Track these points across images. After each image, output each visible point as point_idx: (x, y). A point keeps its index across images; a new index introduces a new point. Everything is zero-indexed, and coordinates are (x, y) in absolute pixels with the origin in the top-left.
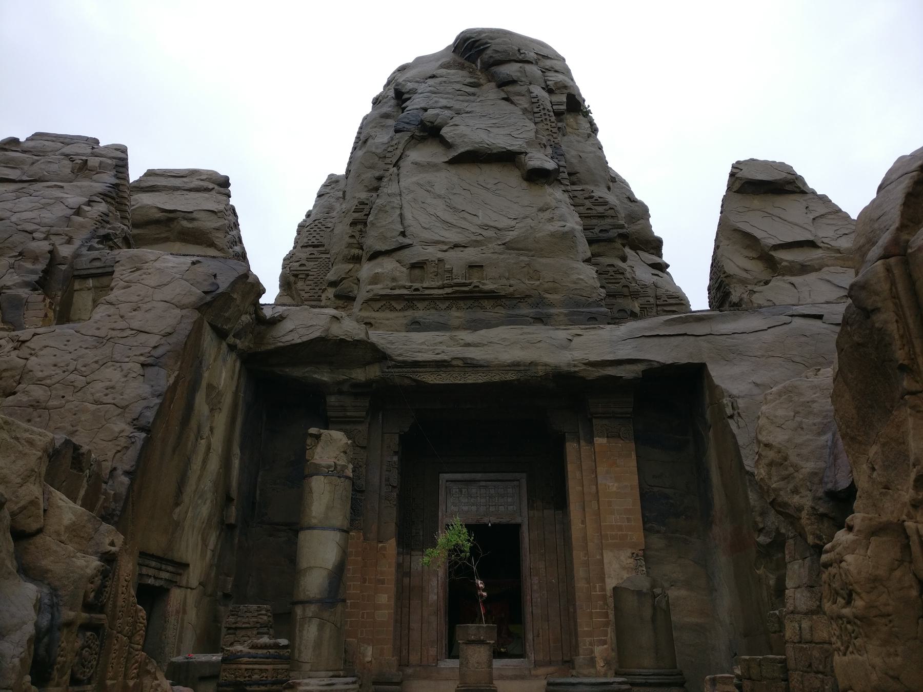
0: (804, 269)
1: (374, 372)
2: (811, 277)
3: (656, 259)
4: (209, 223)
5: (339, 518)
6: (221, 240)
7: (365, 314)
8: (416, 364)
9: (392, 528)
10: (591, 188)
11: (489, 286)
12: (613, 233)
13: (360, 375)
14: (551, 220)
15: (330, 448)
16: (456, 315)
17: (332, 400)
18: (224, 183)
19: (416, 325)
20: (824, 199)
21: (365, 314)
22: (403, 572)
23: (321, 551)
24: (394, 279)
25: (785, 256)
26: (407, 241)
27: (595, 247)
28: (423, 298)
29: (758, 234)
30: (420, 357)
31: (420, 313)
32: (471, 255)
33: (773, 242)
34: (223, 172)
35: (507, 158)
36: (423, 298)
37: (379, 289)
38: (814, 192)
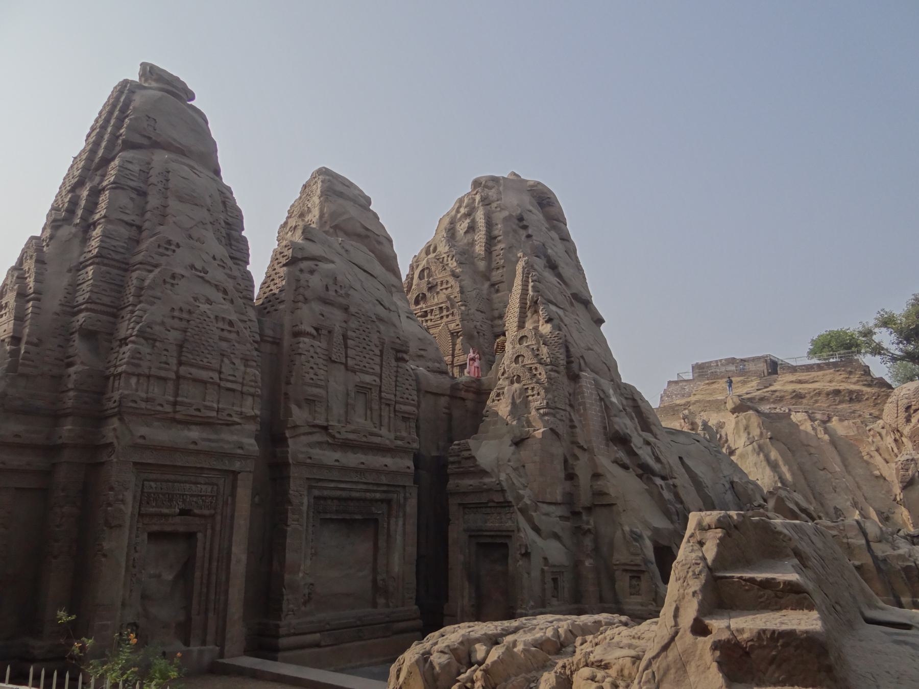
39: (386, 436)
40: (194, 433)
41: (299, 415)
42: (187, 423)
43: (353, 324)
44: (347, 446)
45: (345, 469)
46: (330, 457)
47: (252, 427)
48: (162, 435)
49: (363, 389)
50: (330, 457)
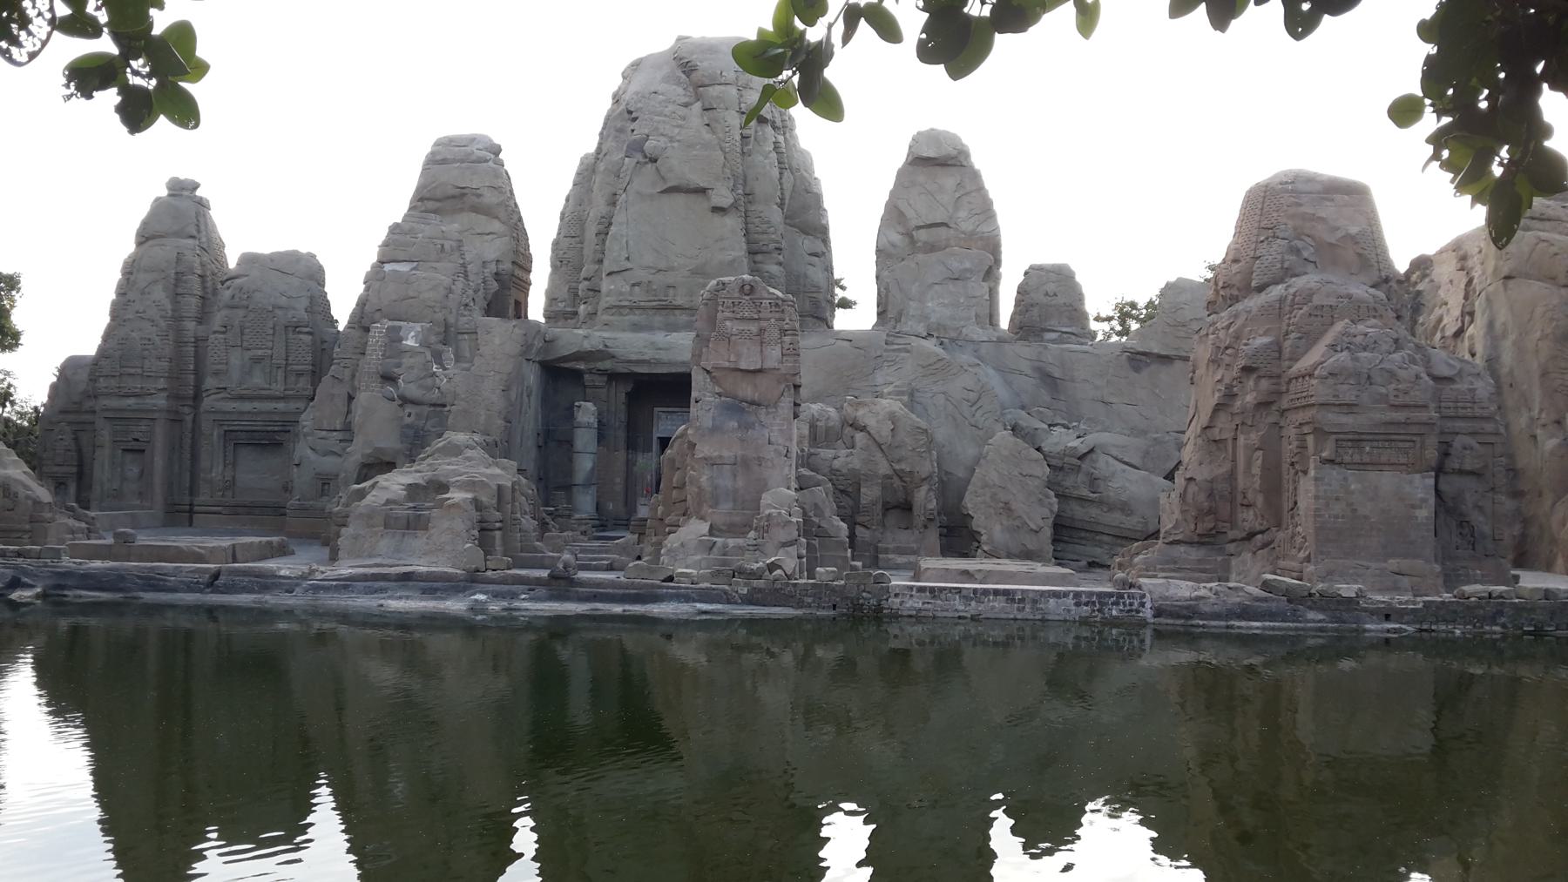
0: (931, 248)
1: (607, 365)
2: (934, 256)
3: (820, 247)
4: (490, 198)
5: (593, 447)
6: (502, 215)
7: (606, 317)
8: (630, 361)
9: (622, 444)
10: (760, 208)
11: (679, 301)
12: (772, 246)
13: (601, 365)
14: (722, 249)
15: (587, 413)
16: (658, 319)
17: (586, 377)
18: (497, 150)
19: (636, 327)
20: (976, 175)
21: (606, 317)
22: (629, 464)
23: (584, 464)
24: (621, 294)
25: (922, 235)
26: (629, 265)
27: (759, 257)
28: (639, 308)
29: (910, 213)
30: (634, 357)
31: (636, 317)
32: (670, 278)
33: (914, 223)
34: (496, 141)
35: (702, 191)
36: (639, 308)
37: (612, 300)
38: (972, 167)
39: (278, 388)
40: (131, 401)
41: (210, 383)
42: (127, 396)
43: (252, 316)
44: (241, 398)
45: (242, 413)
46: (230, 406)
47: (165, 394)
48: (114, 403)
49: (257, 360)
50: (230, 406)
